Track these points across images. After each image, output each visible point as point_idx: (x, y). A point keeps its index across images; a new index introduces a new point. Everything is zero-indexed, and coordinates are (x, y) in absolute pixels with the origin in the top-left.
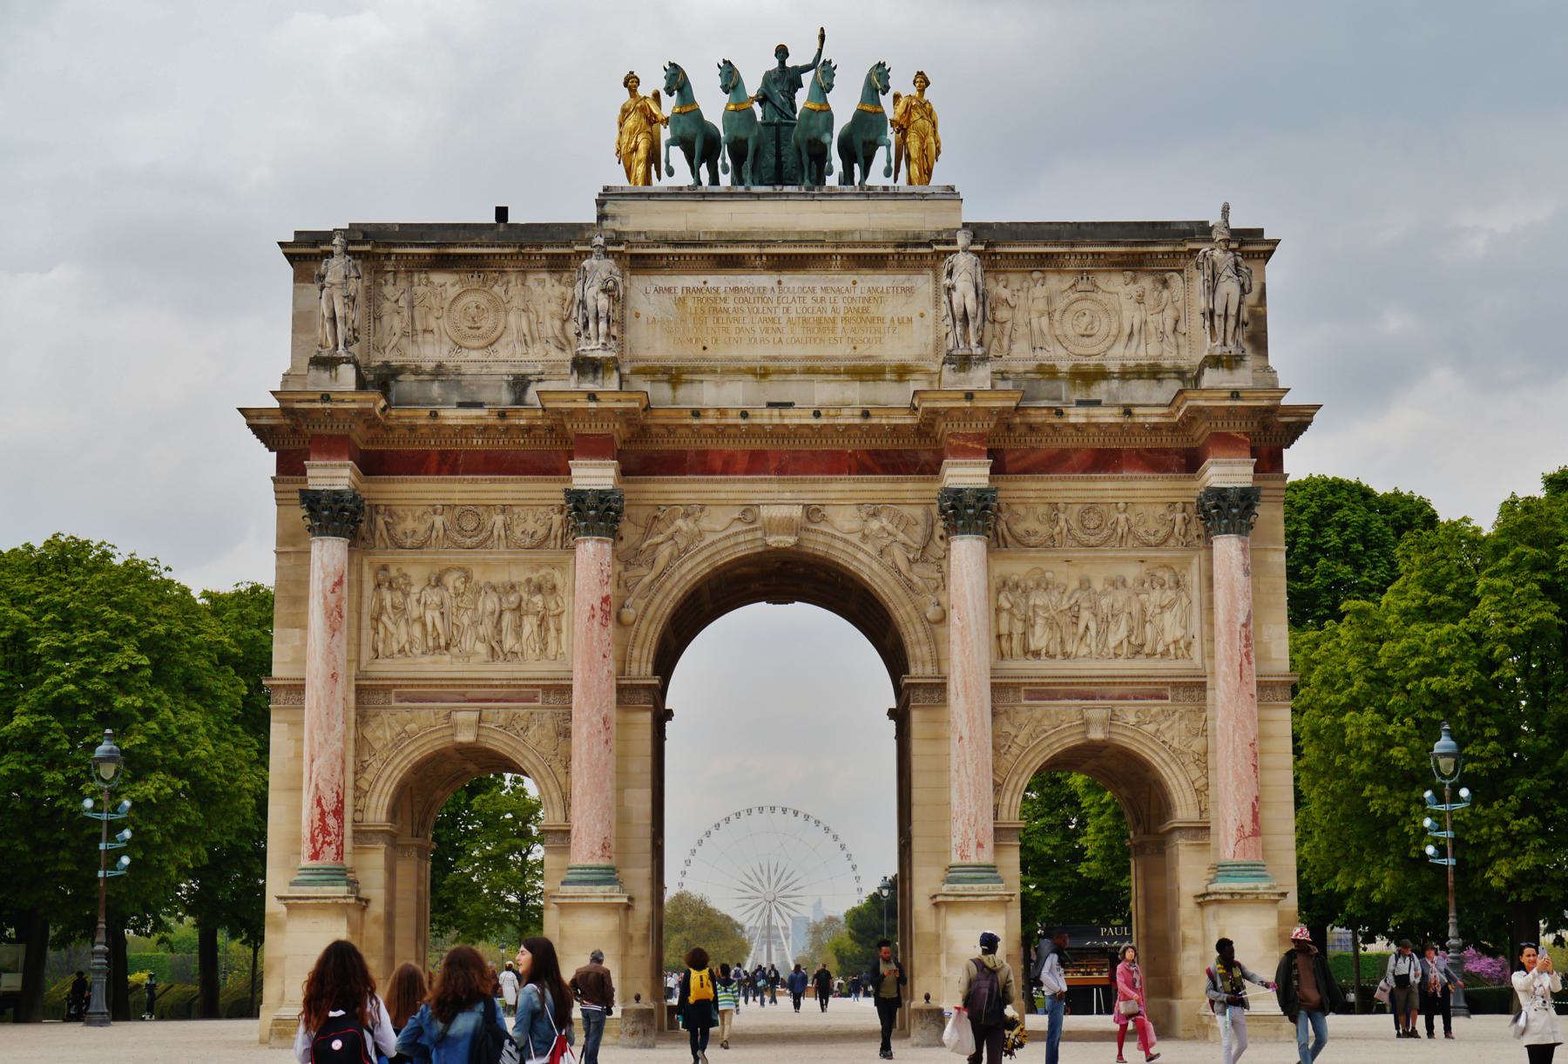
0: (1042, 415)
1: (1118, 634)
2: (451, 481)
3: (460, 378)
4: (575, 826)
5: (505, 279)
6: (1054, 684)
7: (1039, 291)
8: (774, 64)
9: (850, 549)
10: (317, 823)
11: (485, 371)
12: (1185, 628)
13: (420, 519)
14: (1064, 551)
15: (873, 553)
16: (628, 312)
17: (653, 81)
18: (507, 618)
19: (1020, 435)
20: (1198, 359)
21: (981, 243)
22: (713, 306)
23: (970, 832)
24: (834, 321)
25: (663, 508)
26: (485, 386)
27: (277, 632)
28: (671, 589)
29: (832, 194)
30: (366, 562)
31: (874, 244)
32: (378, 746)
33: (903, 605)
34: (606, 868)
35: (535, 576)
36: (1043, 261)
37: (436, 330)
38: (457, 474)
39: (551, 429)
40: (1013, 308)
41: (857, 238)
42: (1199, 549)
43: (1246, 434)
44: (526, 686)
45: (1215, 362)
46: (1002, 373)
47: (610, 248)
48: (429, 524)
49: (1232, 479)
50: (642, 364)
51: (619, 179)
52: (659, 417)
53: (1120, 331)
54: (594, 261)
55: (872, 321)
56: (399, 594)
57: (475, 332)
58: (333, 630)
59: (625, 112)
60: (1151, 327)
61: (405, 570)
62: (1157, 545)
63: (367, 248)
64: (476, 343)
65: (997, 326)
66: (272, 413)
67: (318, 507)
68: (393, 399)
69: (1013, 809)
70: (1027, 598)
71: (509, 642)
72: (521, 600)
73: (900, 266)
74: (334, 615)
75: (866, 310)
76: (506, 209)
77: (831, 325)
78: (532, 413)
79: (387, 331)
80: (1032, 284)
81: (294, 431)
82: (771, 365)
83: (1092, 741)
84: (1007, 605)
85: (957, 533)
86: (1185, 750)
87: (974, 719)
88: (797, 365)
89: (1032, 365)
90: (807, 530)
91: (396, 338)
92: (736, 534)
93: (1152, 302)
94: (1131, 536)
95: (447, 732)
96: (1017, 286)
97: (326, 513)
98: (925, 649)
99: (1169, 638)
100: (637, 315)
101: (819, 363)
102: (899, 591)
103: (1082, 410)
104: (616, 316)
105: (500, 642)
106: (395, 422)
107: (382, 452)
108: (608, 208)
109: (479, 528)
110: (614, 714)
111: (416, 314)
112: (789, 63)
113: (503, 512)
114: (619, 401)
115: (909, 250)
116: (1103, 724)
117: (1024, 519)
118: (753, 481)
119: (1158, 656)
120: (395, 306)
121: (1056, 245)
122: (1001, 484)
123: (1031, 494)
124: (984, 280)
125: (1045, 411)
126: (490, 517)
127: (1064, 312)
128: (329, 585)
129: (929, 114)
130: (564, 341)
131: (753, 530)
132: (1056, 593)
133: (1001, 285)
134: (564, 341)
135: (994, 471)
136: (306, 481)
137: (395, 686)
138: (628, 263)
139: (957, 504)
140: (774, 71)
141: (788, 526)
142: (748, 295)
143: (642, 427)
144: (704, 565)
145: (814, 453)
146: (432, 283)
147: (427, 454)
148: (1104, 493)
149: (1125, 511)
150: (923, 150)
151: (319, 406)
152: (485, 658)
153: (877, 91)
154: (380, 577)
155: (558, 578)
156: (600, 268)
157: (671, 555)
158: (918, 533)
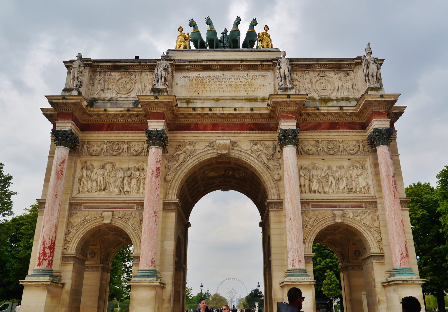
0: (312, 110)
1: (343, 185)
2: (111, 133)
3: (117, 101)
4: (141, 253)
5: (135, 74)
6: (322, 202)
7: (307, 76)
9: (247, 156)
10: (42, 252)
11: (125, 99)
12: (367, 182)
13: (99, 146)
14: (322, 156)
16: (174, 83)
18: (126, 179)
19: (304, 118)
22: (202, 81)
23: (296, 256)
24: (241, 85)
25: (182, 142)
26: (125, 104)
28: (184, 169)
30: (79, 160)
31: (253, 61)
32: (75, 224)
33: (266, 175)
34: (152, 271)
35: (137, 166)
37: (111, 89)
40: (299, 81)
42: (369, 155)
44: (131, 203)
48: (102, 148)
52: (181, 111)
56: (89, 171)
59: (178, 37)
60: (345, 87)
61: (92, 163)
62: (354, 154)
64: (124, 92)
69: (309, 249)
70: (310, 172)
71: (126, 188)
73: (262, 69)
76: (138, 56)
77: (240, 87)
78: (138, 110)
79: (96, 89)
80: (305, 75)
82: (220, 98)
83: (337, 223)
84: (303, 175)
85: (286, 145)
86: (372, 226)
87: (295, 212)
88: (228, 98)
91: (98, 91)
92: (207, 150)
93: (344, 80)
95: (101, 220)
98: (274, 190)
99: (361, 186)
102: (265, 170)
105: (123, 188)
107: (89, 124)
108: (170, 54)
109: (119, 149)
110: (161, 213)
111: (106, 84)
113: (128, 143)
114: (165, 99)
115: (265, 63)
116: (341, 216)
117: (307, 146)
118: (213, 133)
119: (358, 192)
120: (99, 81)
123: (309, 137)
125: (313, 108)
126: (123, 145)
129: (268, 36)
132: (320, 171)
133: (295, 74)
137: (83, 203)
138: (174, 68)
141: (225, 147)
142: (213, 78)
145: (234, 124)
146: (112, 75)
147: (103, 125)
148: (334, 137)
157: (184, 157)
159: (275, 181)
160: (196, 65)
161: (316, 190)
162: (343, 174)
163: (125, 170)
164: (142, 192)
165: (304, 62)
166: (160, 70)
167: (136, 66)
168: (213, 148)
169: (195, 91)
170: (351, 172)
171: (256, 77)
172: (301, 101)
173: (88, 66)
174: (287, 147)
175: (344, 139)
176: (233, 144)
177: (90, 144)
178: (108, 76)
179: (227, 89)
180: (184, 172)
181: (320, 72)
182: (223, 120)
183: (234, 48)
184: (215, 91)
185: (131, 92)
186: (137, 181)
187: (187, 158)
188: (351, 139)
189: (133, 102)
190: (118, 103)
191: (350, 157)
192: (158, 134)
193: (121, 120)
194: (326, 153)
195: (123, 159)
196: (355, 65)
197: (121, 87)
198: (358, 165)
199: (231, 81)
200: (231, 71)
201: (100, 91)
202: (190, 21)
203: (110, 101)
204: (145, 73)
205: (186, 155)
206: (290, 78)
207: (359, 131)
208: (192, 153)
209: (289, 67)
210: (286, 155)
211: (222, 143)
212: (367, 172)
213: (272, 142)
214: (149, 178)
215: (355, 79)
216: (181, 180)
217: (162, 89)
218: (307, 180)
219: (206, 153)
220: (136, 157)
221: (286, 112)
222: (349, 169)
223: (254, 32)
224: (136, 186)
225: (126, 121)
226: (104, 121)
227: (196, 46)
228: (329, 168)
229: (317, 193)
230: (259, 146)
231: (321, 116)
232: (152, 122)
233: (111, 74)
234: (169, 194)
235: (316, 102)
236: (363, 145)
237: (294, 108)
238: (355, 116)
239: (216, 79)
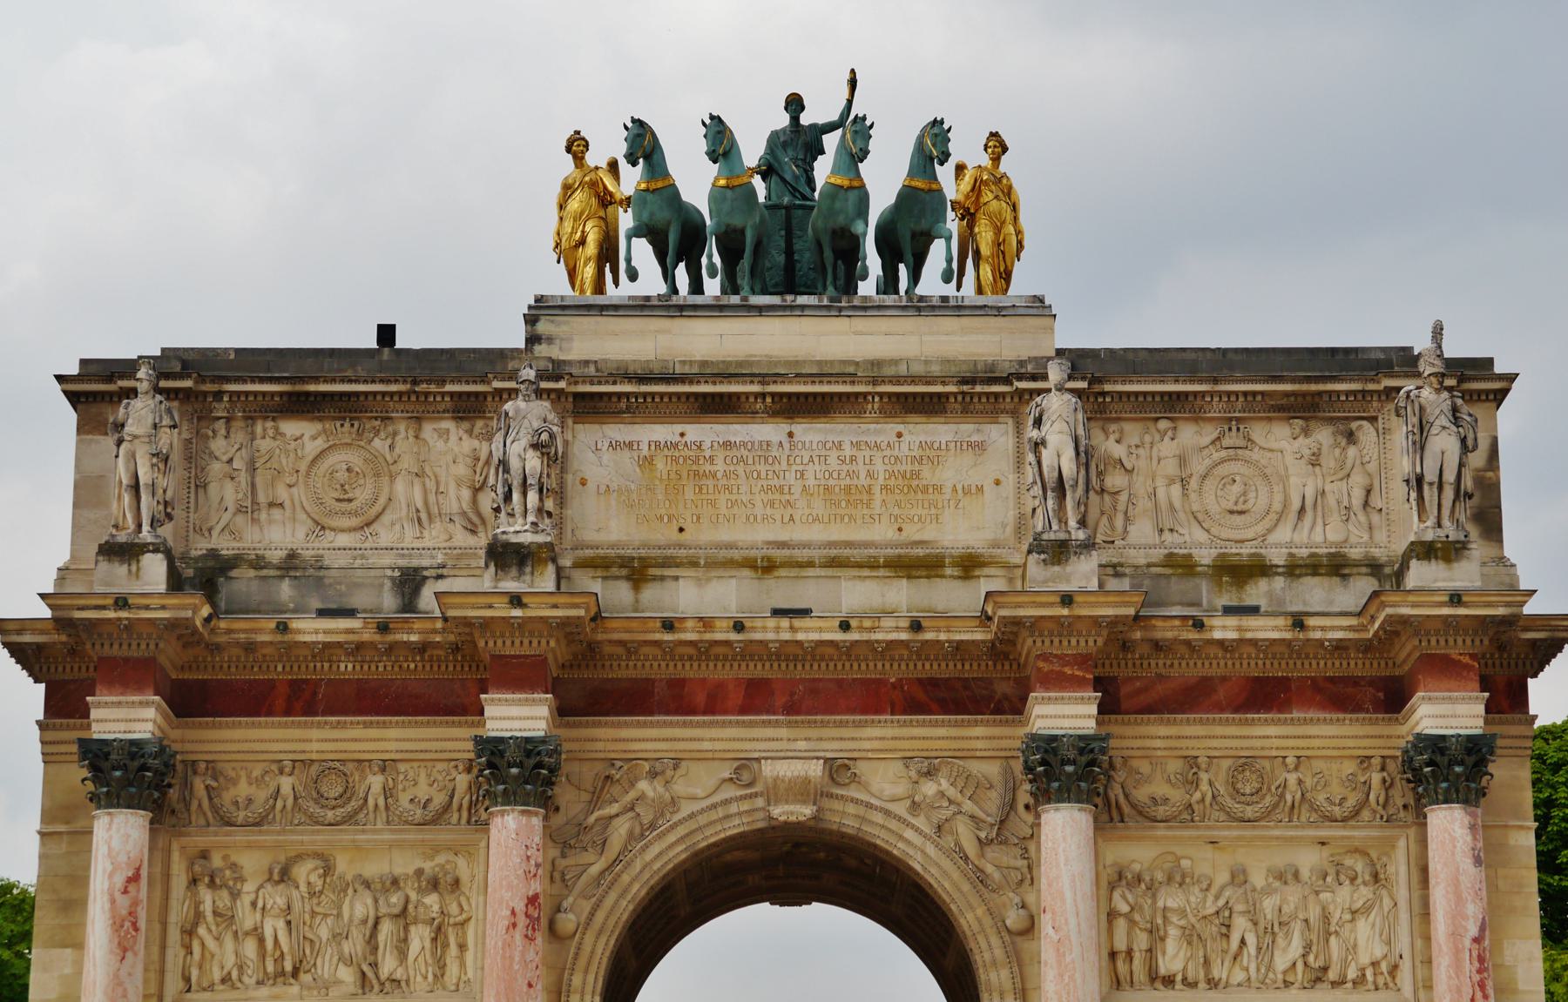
0: (1172, 629)
1: (1288, 952)
2: (306, 725)
3: (323, 572)
5: (390, 429)
7: (1167, 448)
8: (784, 120)
9: (893, 825)
11: (358, 562)
12: (1389, 943)
13: (259, 782)
14: (1209, 828)
15: (927, 831)
16: (569, 478)
17: (608, 145)
18: (386, 928)
19: (1141, 658)
20: (1400, 547)
21: (1083, 379)
22: (693, 468)
24: (869, 491)
25: (618, 764)
26: (358, 585)
27: (37, 955)
28: (630, 884)
29: (866, 308)
31: (928, 380)
33: (972, 908)
35: (428, 866)
36: (1173, 403)
37: (287, 504)
38: (315, 714)
39: (456, 648)
41: (902, 370)
43: (1473, 656)
45: (1426, 551)
46: (1114, 566)
47: (544, 385)
48: (272, 789)
49: (1454, 722)
50: (589, 553)
51: (557, 285)
52: (614, 630)
53: (1286, 504)
54: (520, 403)
55: (925, 490)
56: (225, 893)
57: (344, 505)
58: (123, 949)
59: (568, 189)
60: (1331, 500)
61: (234, 858)
63: (188, 383)
65: (1107, 497)
66: (39, 626)
67: (105, 765)
68: (223, 605)
70: (1154, 897)
71: (388, 965)
72: (407, 901)
73: (965, 411)
74: (125, 928)
77: (865, 497)
78: (428, 625)
79: (215, 505)
80: (1157, 437)
81: (73, 652)
82: (778, 554)
84: (1125, 908)
85: (1049, 801)
88: (816, 554)
89: (1158, 554)
90: (831, 796)
92: (726, 802)
93: (1332, 464)
94: (1306, 806)
96: (1136, 441)
97: (118, 773)
98: (1005, 973)
99: (1364, 959)
100: (583, 483)
101: (847, 552)
102: (966, 887)
103: (1232, 621)
104: (552, 483)
105: (374, 965)
106: (222, 639)
107: (204, 681)
108: (542, 327)
109: (346, 794)
111: (258, 480)
112: (806, 119)
113: (383, 770)
114: (555, 606)
115: (978, 388)
117: (1148, 780)
118: (751, 724)
119: (1349, 985)
120: (227, 468)
121: (1192, 382)
122: (1115, 729)
123: (1158, 743)
124: (1088, 431)
125: (1177, 623)
126: (363, 778)
127: (1204, 477)
128: (119, 881)
130: (475, 519)
131: (751, 796)
132: (1196, 890)
133: (1112, 438)
134: (475, 519)
135: (1102, 710)
136: (89, 727)
138: (570, 406)
139: (1050, 758)
140: (784, 130)
141: (801, 790)
142: (745, 453)
143: (589, 644)
144: (680, 848)
145: (840, 683)
146: (283, 435)
147: (271, 685)
148: (1267, 743)
149: (1296, 768)
150: (998, 244)
151: (111, 614)
152: (352, 989)
153: (932, 159)
154: (197, 868)
155: (463, 868)
156: (529, 413)
157: (631, 835)
158: (993, 801)
159: (1007, 938)
160: (670, 395)
161: (1174, 975)
162: (1292, 906)
163: (379, 886)
164: (454, 981)
165: (1154, 382)
167: (396, 398)
168: (749, 791)
169: (666, 520)
170: (1325, 896)
171: (939, 448)
173: (176, 398)
174: (1057, 809)
175: (1309, 753)
176: (836, 771)
177: (221, 773)
178: (268, 439)
179: (809, 506)
180: (629, 897)
181: (1226, 427)
182: (791, 666)
184: (755, 518)
185: (380, 514)
186: (433, 935)
187: (643, 835)
188: (1335, 753)
189: (392, 579)
190: (327, 581)
191: (1323, 833)
192: (528, 754)
193: (350, 666)
194: (1228, 814)
195: (368, 841)
196: (1383, 398)
197: (329, 496)
198: (1359, 867)
200: (825, 420)
201: (235, 514)
202: (626, 128)
203: (292, 573)
204: (435, 426)
205: (637, 824)
207: (1370, 719)
208: (662, 814)
210: (1050, 844)
211: (789, 774)
212: (1393, 899)
213: (998, 763)
214: (500, 944)
215: (1383, 461)
216: (617, 933)
217: (533, 547)
218: (1140, 929)
219: (721, 812)
220: (422, 830)
221: (1056, 656)
222: (1321, 882)
224: (428, 956)
225: (373, 668)
226: (272, 668)
228: (1236, 881)
229: (1182, 987)
230: (945, 784)
231: (1213, 651)
232: (500, 700)
233: (277, 429)
234: (569, 991)
235: (1197, 581)
236: (1384, 781)
237: (1091, 643)
238: (1358, 651)
239: (757, 459)
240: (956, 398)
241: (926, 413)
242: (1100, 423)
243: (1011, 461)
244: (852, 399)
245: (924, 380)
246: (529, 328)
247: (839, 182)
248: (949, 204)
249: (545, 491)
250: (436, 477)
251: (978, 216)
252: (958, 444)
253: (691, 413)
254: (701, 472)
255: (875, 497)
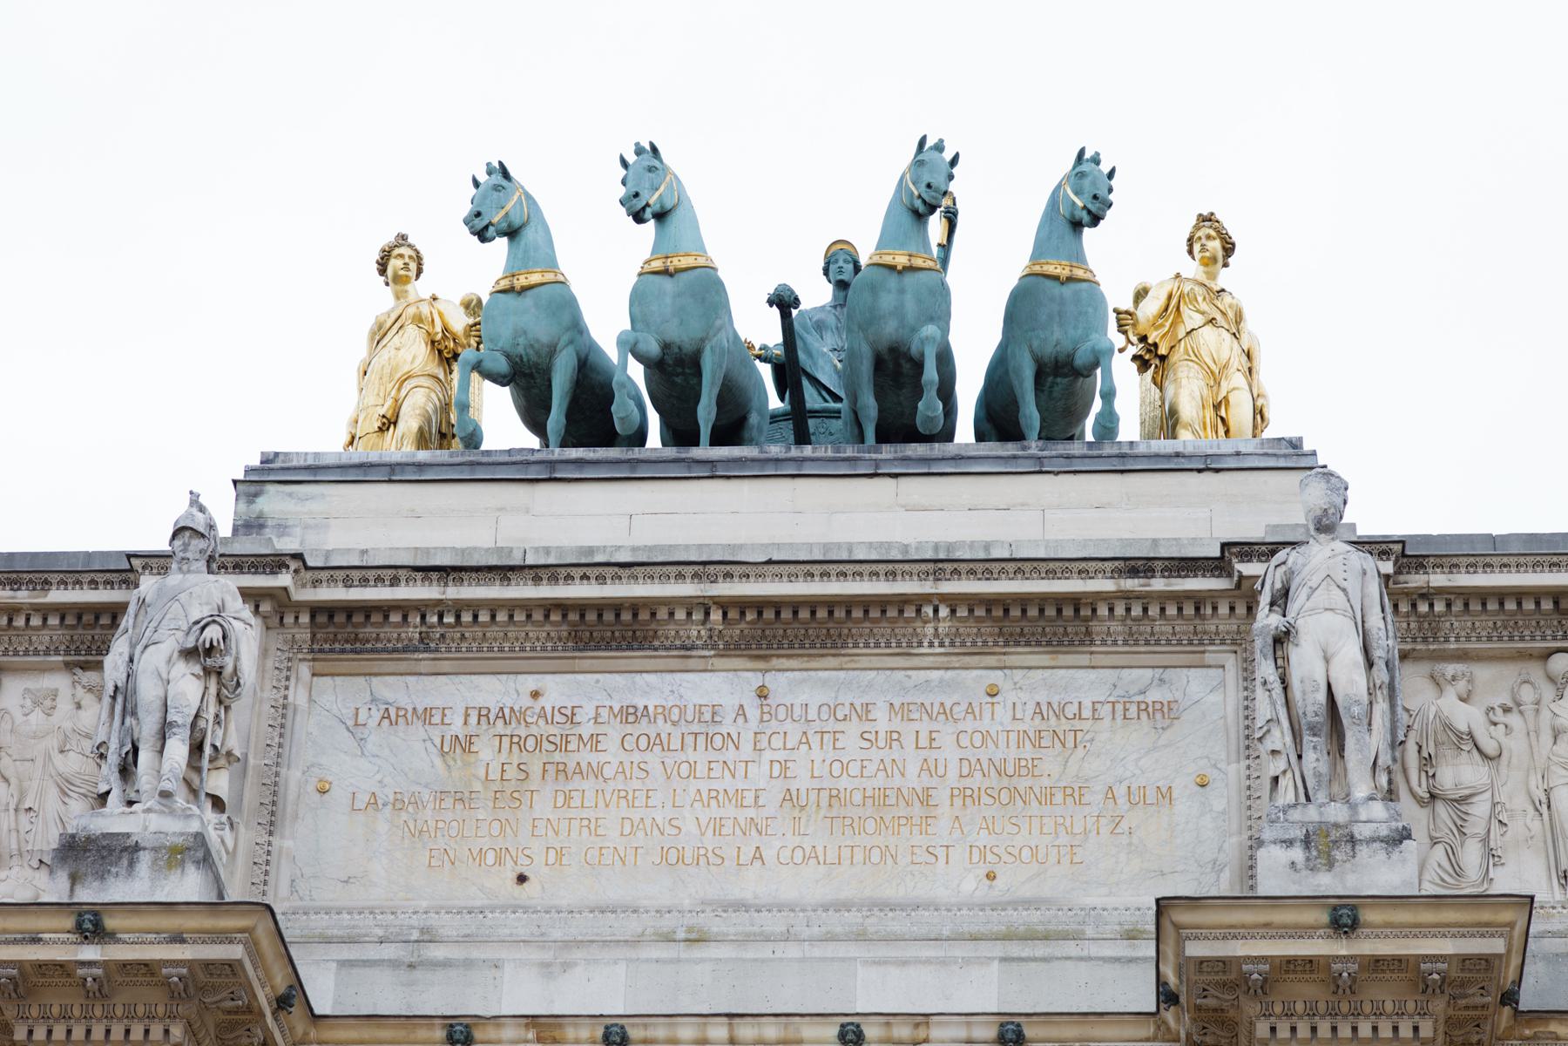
24: (925, 798)
55: (1047, 797)
59: (380, 335)
65: (1441, 809)
73: (1131, 639)
75: (1028, 768)
77: (917, 810)
80: (1548, 692)
114: (178, 938)
115: (1158, 584)
138: (304, 635)
142: (663, 727)
160: (512, 606)
166: (155, 659)
171: (1079, 716)
172: (1464, 959)
183: (884, 436)
184: (680, 859)
199: (831, 755)
202: (476, 184)
206: (1378, 739)
209: (1375, 621)
223: (1080, 284)
227: (534, 414)
239: (689, 740)
240: (1111, 610)
241: (1049, 643)
242: (1424, 668)
243: (1233, 735)
244: (892, 613)
245: (1043, 566)
246: (242, 506)
247: (888, 260)
248: (1112, 317)
249: (208, 750)
250: (20, 781)
251: (1173, 358)
252: (1119, 707)
253: (554, 649)
254: (571, 766)
255: (939, 811)
